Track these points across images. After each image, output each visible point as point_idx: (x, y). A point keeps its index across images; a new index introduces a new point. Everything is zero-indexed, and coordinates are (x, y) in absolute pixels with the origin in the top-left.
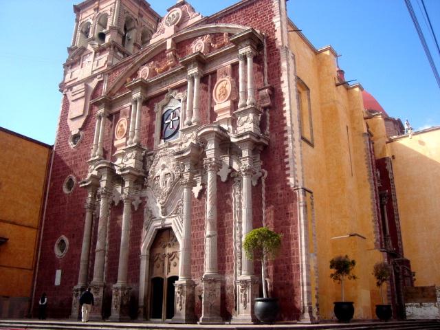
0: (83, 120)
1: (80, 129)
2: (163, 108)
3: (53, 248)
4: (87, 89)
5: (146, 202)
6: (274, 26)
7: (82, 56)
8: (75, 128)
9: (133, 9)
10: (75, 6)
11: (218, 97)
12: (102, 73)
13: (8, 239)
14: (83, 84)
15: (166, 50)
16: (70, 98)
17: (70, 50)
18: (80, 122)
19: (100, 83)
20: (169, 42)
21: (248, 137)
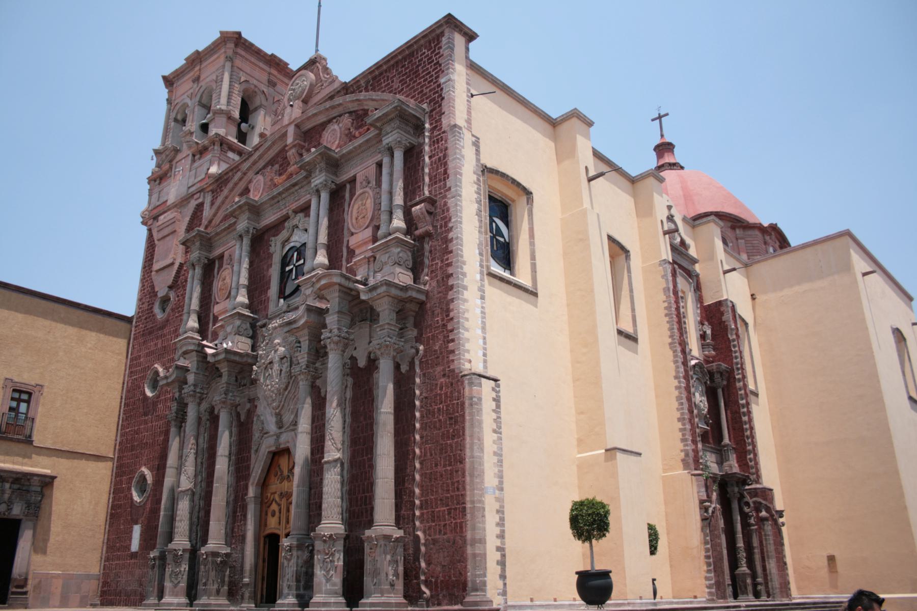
1: (170, 287)
2: (283, 247)
3: (129, 489)
5: (256, 407)
6: (442, 89)
7: (174, 163)
8: (162, 284)
9: (257, 74)
10: (164, 78)
11: (354, 221)
12: (201, 191)
15: (286, 146)
16: (156, 236)
17: (157, 152)
20: (291, 130)
21: (384, 288)
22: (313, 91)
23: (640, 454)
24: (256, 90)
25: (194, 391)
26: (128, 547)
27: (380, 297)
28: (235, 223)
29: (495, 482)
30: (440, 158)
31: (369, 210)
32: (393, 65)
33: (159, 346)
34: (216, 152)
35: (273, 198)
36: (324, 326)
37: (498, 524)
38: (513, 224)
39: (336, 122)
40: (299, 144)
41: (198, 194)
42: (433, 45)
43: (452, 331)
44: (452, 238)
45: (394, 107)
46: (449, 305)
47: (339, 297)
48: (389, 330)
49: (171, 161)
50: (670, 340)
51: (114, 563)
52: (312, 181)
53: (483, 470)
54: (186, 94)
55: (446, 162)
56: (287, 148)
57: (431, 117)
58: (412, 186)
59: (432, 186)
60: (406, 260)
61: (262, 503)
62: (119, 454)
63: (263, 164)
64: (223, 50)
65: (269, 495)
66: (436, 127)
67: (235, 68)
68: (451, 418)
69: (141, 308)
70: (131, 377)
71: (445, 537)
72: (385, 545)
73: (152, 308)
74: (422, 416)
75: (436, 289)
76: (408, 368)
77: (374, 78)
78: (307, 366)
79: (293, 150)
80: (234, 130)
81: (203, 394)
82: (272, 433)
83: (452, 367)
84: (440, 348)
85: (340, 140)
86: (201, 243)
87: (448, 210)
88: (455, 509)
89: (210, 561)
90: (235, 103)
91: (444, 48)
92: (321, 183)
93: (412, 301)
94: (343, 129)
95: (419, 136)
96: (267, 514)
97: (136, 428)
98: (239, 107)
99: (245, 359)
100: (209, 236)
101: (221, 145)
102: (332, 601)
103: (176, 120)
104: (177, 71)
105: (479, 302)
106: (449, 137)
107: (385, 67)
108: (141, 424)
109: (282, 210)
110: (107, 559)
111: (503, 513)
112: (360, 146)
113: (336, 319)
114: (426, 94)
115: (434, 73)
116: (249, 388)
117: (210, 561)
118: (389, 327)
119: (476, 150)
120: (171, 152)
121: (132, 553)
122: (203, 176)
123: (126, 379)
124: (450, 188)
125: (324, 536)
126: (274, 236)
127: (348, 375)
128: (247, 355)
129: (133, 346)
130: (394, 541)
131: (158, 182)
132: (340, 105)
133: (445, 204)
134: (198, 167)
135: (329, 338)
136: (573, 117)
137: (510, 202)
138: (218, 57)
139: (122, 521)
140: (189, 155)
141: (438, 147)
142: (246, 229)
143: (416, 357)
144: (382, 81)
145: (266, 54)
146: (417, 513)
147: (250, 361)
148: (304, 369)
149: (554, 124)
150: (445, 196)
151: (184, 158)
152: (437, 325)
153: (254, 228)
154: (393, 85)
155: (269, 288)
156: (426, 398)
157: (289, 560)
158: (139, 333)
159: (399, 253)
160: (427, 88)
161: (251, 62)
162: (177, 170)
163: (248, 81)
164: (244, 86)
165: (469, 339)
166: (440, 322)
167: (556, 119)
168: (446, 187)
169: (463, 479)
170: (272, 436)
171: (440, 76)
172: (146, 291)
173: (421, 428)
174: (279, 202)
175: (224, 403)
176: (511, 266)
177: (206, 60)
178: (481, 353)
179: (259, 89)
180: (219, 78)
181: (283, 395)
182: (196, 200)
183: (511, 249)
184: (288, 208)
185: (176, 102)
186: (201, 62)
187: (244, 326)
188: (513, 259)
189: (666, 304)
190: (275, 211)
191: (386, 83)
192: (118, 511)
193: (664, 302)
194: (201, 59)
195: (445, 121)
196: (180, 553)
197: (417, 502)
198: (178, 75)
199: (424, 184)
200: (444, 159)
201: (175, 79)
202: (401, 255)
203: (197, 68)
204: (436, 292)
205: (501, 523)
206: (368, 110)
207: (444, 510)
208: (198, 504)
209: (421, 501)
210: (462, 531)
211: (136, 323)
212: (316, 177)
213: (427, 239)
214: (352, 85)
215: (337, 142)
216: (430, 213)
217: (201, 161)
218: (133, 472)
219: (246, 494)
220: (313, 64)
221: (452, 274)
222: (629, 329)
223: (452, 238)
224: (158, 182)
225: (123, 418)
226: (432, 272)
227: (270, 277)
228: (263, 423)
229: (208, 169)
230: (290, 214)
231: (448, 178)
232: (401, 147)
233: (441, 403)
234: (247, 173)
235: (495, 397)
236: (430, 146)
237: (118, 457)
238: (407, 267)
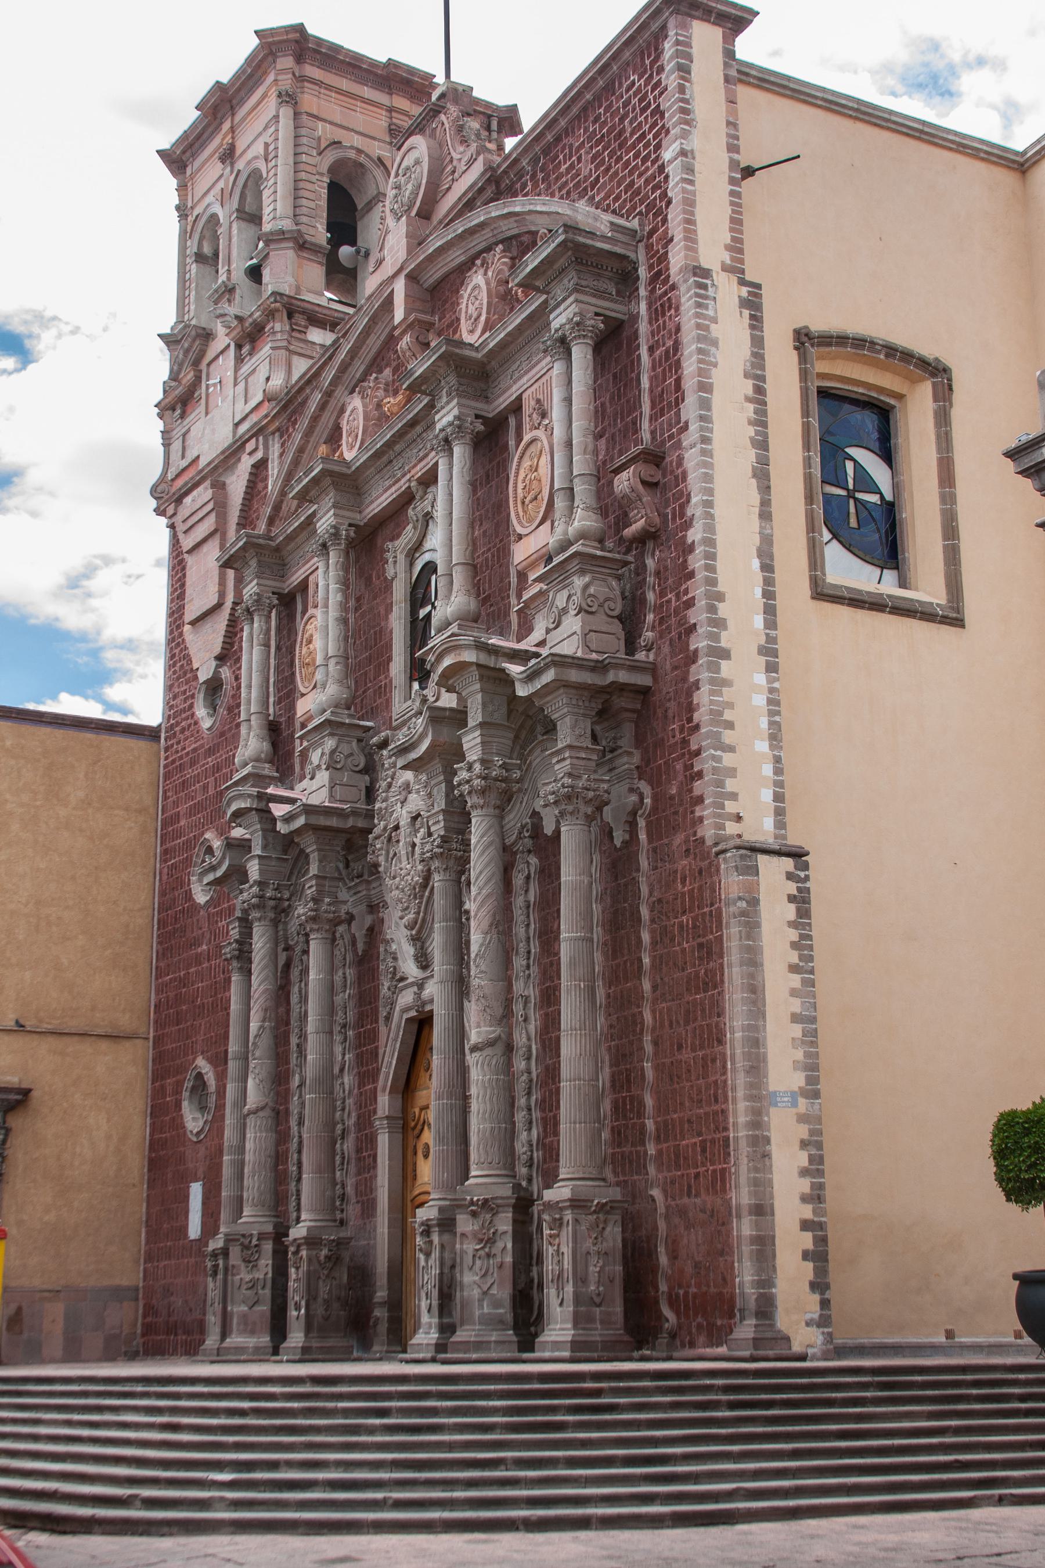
0: (220, 623)
1: (221, 658)
3: (178, 1105)
4: (220, 506)
5: (382, 920)
6: (667, 177)
7: (203, 366)
12: (258, 432)
13: (30, 1090)
14: (208, 483)
17: (169, 340)
18: (214, 635)
19: (260, 467)
20: (400, 287)
22: (438, 186)
24: (362, 159)
25: (261, 897)
26: (184, 1228)
27: (547, 690)
28: (314, 514)
29: (798, 1080)
30: (667, 352)
31: (543, 480)
32: (578, 117)
33: (211, 791)
34: (279, 336)
35: (377, 455)
36: (461, 756)
37: (804, 1172)
38: (900, 457)
39: (482, 265)
40: (419, 321)
41: (254, 440)
42: (647, 62)
43: (698, 753)
44: (694, 541)
45: (559, 245)
46: (691, 696)
47: (482, 690)
48: (575, 761)
49: (196, 363)
51: (162, 1264)
52: (437, 417)
53: (765, 1055)
54: (212, 193)
55: (678, 362)
56: (396, 333)
57: (649, 247)
58: (622, 420)
59: (656, 420)
60: (607, 600)
61: (405, 1128)
62: (156, 1031)
63: (362, 368)
64: (271, 78)
65: (417, 1110)
66: (659, 274)
67: (304, 117)
68: (701, 946)
69: (171, 707)
70: (166, 861)
71: (698, 1201)
72: (576, 1220)
73: (191, 706)
74: (654, 943)
75: (668, 658)
76: (627, 837)
77: (546, 151)
78: (445, 839)
79: (407, 339)
80: (315, 273)
81: (281, 899)
82: (410, 980)
83: (699, 834)
84: (679, 793)
85: (488, 313)
86: (259, 561)
87: (684, 478)
88: (713, 1141)
89: (304, 1256)
90: (312, 205)
91: (667, 69)
92: (450, 424)
93: (622, 690)
94: (493, 284)
95: (629, 297)
96: (415, 1153)
97: (182, 973)
98: (325, 215)
99: (350, 822)
100: (273, 544)
101: (290, 316)
102: (493, 1339)
103: (200, 258)
104: (186, 134)
105: (761, 679)
106: (683, 300)
107: (563, 123)
108: (189, 966)
109: (399, 480)
110: (149, 1258)
111: (819, 1145)
112: (520, 328)
113: (479, 740)
114: (638, 192)
115: (651, 136)
116: (368, 882)
117: (304, 1256)
118: (574, 754)
119: (752, 317)
120: (194, 341)
121: (192, 1241)
122: (259, 397)
123: (158, 865)
124: (686, 427)
125: (472, 1203)
126: (393, 539)
127: (529, 851)
128: (354, 813)
129: (165, 792)
130: (595, 1212)
131: (178, 412)
132: (482, 226)
133: (680, 460)
134: (249, 375)
135: (468, 782)
137: (892, 402)
138: (264, 96)
139: (170, 1175)
140: (229, 345)
141: (664, 322)
142: (332, 531)
143: (640, 812)
144: (561, 157)
145: (374, 64)
146: (651, 1149)
147: (361, 823)
148: (437, 847)
149: (1022, 165)
150: (678, 445)
151: (222, 352)
152: (672, 741)
153: (350, 525)
154: (580, 168)
155: (390, 659)
156: (660, 901)
157: (428, 1255)
158: (174, 761)
159: (586, 587)
160: (640, 175)
161: (340, 91)
162: (211, 382)
163: (340, 143)
164: (331, 157)
165: (735, 770)
166: (677, 733)
167: (1025, 152)
168: (679, 422)
169: (723, 1078)
170: (412, 984)
171: (663, 142)
172: (177, 668)
173: (653, 965)
174: (391, 461)
175: (314, 919)
176: (900, 557)
177: (242, 102)
178: (767, 795)
179: (367, 155)
180: (271, 148)
181: (422, 897)
182: (250, 454)
183: (897, 518)
184: (408, 477)
185: (195, 213)
186: (232, 108)
187: (345, 749)
190: (387, 483)
191: (568, 163)
192: (162, 1153)
194: (230, 101)
195: (677, 259)
196: (254, 1242)
197: (650, 1125)
198: (191, 145)
199: (641, 413)
200: (674, 355)
201: (188, 154)
202: (592, 590)
203: (226, 126)
204: (668, 667)
205: (815, 1168)
206: (537, 232)
207: (695, 1143)
208: (296, 1134)
209: (656, 1123)
210: (724, 1190)
211: (166, 740)
212: (443, 408)
213: (650, 545)
214: (505, 172)
215: (483, 318)
216: (650, 485)
217: (253, 360)
218: (182, 1069)
219: (375, 1112)
220: (435, 116)
221: (695, 625)
223: (694, 541)
224: (178, 412)
225: (157, 953)
226: (662, 621)
227: (391, 632)
228: (395, 959)
229: (268, 379)
230: (414, 489)
231: (683, 400)
233: (684, 913)
234: (333, 391)
235: (795, 892)
236: (650, 323)
237: (154, 1037)
238: (609, 616)
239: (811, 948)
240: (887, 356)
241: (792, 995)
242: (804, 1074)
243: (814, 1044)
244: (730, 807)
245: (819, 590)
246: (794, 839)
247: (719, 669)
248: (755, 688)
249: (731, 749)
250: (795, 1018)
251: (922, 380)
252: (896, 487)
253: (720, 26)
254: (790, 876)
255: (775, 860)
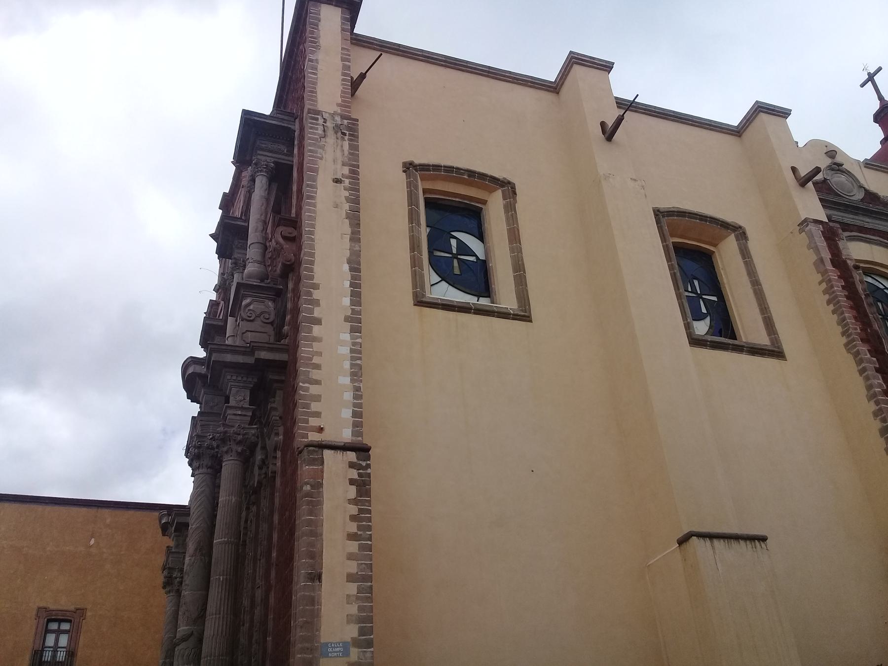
23: (763, 539)
29: (352, 632)
50: (844, 340)
105: (346, 337)
136: (572, 67)
165: (320, 396)
188: (492, 277)
189: (824, 285)
193: (820, 283)
222: (762, 339)
232: (261, 171)
235: (356, 477)
239: (369, 520)
240: (469, 176)
241: (349, 559)
242: (357, 626)
243: (370, 599)
244: (313, 422)
245: (419, 299)
246: (367, 441)
247: (312, 330)
248: (342, 343)
249: (317, 382)
250: (351, 578)
251: (495, 190)
252: (487, 252)
253: (339, 7)
254: (352, 465)
255: (339, 454)
